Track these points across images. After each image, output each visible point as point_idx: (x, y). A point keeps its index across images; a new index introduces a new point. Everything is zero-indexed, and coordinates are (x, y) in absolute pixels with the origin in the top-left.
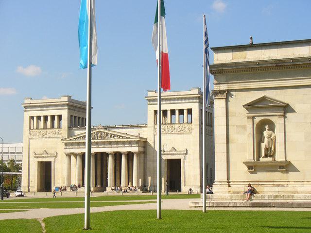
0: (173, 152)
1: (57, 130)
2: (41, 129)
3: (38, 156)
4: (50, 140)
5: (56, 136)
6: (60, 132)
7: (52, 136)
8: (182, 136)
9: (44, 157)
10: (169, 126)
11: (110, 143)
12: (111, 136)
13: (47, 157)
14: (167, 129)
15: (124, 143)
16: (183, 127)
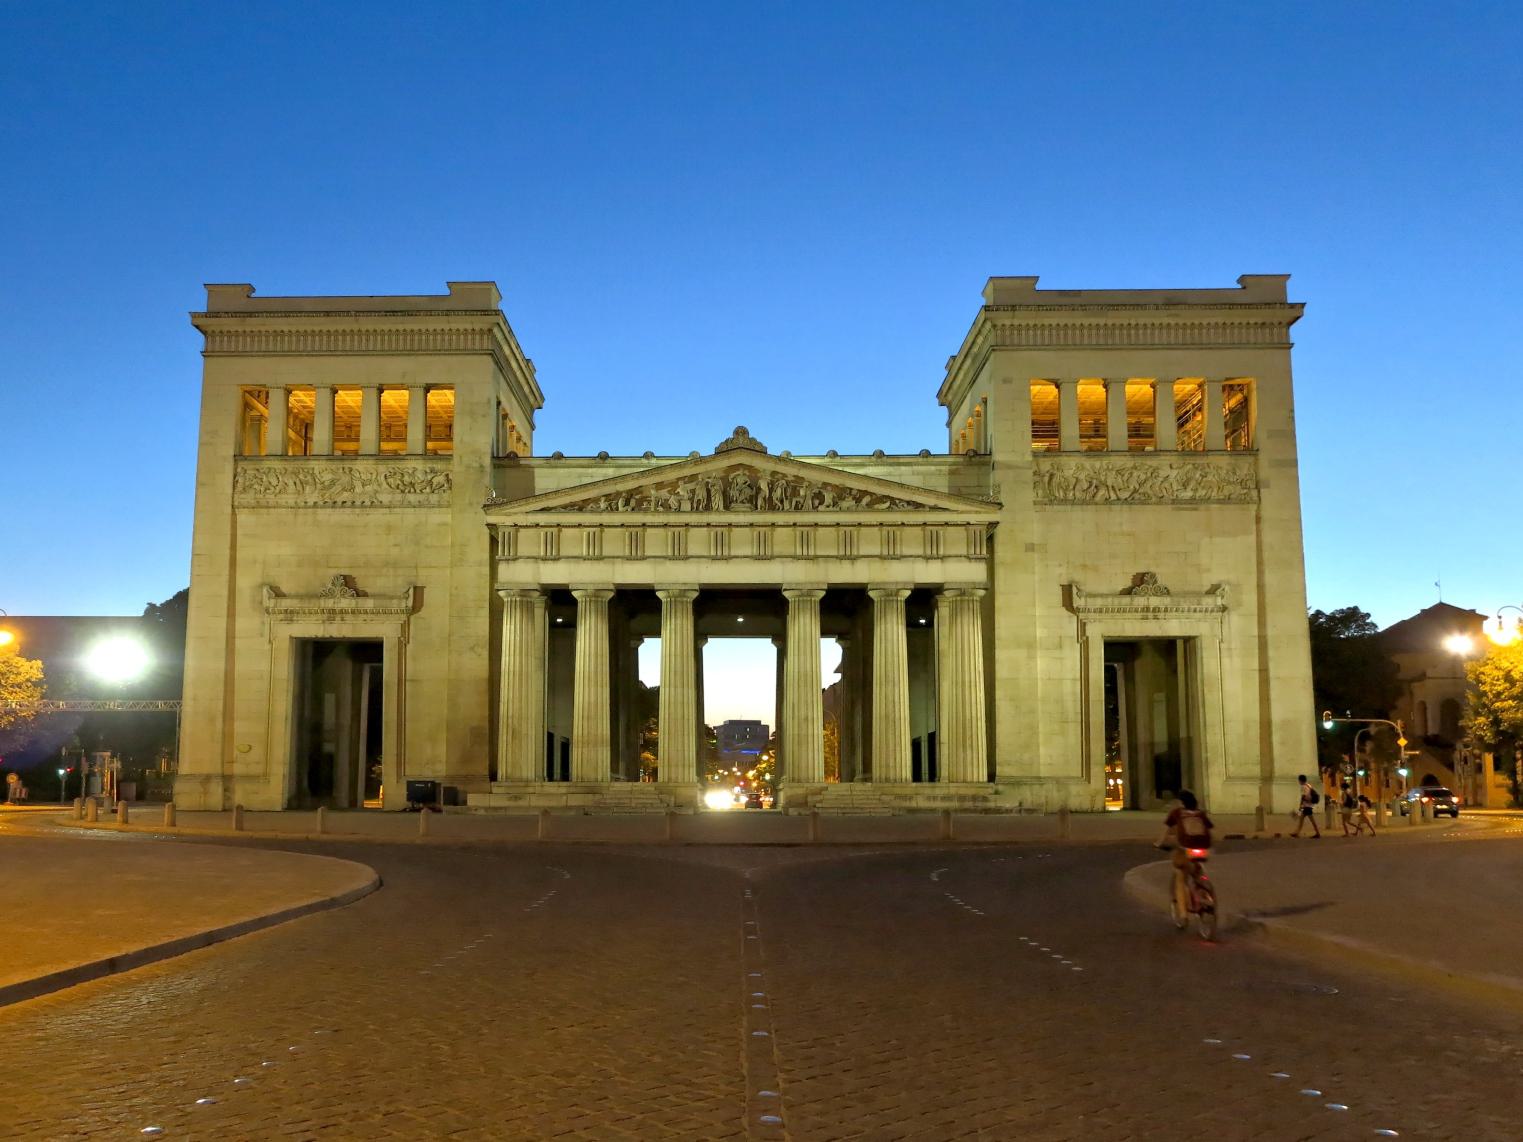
2: (318, 457)
4: (377, 516)
5: (412, 498)
7: (385, 498)
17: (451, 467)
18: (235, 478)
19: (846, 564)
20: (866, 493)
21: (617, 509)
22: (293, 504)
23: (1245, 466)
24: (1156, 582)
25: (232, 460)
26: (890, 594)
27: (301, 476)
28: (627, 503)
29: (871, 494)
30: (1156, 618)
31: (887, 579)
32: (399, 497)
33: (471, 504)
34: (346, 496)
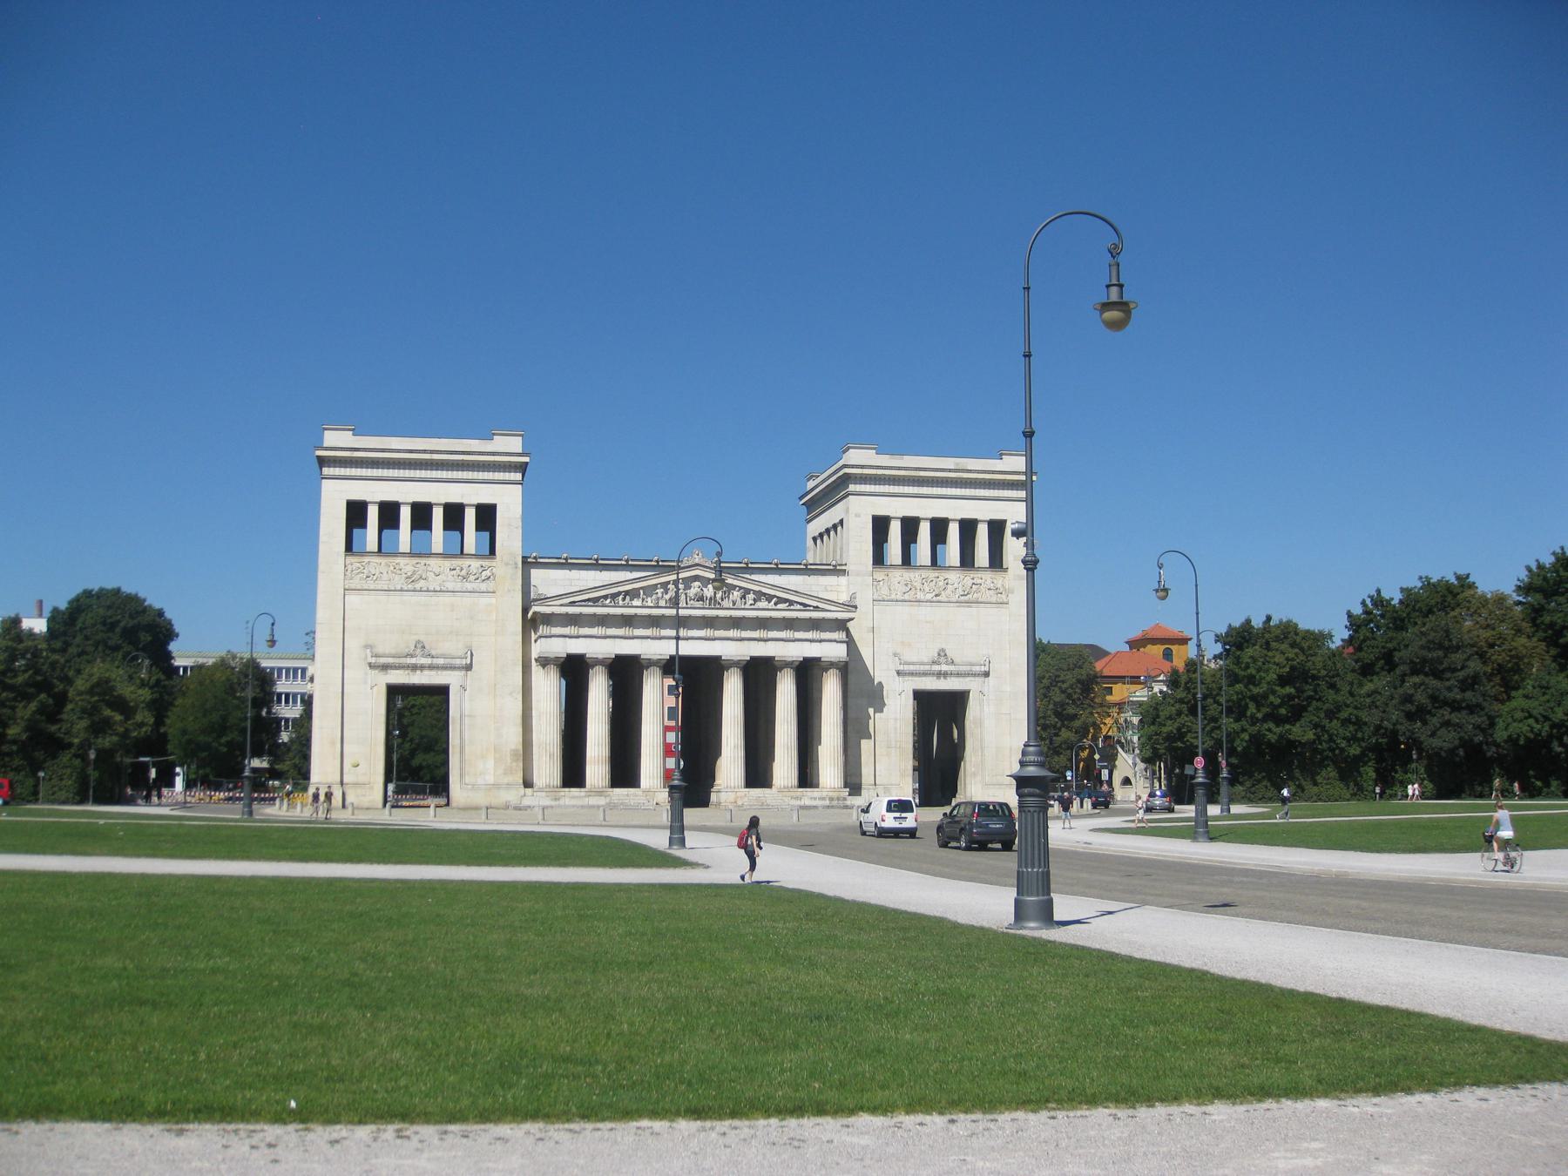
0: (944, 668)
1: (475, 564)
2: (403, 554)
3: (391, 660)
5: (469, 586)
6: (488, 573)
7: (450, 586)
8: (974, 610)
9: (414, 668)
10: (925, 573)
11: (737, 623)
12: (743, 597)
13: (431, 667)
14: (918, 585)
15: (789, 624)
16: (979, 581)
17: (494, 564)
18: (345, 566)
19: (762, 643)
20: (775, 596)
21: (618, 603)
22: (386, 589)
23: (998, 579)
24: (946, 655)
25: (343, 554)
26: (787, 664)
27: (392, 568)
28: (624, 599)
29: (778, 597)
30: (945, 678)
31: (786, 655)
32: (459, 585)
33: (509, 591)
34: (421, 584)
